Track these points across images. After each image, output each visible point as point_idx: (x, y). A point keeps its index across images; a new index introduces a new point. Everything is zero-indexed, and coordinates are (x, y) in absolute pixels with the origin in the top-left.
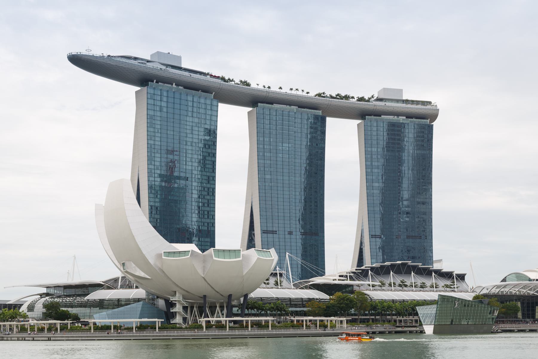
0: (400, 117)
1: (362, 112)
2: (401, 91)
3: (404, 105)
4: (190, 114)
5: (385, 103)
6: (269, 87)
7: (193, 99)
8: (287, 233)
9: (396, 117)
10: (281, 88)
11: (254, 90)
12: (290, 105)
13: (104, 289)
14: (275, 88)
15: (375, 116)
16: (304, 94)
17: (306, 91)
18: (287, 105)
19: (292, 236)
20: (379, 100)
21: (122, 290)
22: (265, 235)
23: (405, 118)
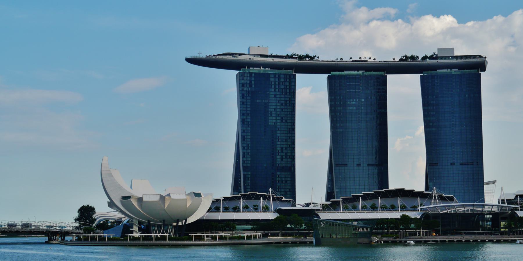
0: (453, 70)
2: (452, 50)
3: (454, 61)
4: (273, 86)
5: (438, 60)
6: (342, 59)
9: (449, 70)
10: (351, 58)
14: (346, 59)
15: (432, 70)
16: (372, 60)
17: (372, 58)
18: (355, 70)
19: (360, 168)
23: (457, 70)
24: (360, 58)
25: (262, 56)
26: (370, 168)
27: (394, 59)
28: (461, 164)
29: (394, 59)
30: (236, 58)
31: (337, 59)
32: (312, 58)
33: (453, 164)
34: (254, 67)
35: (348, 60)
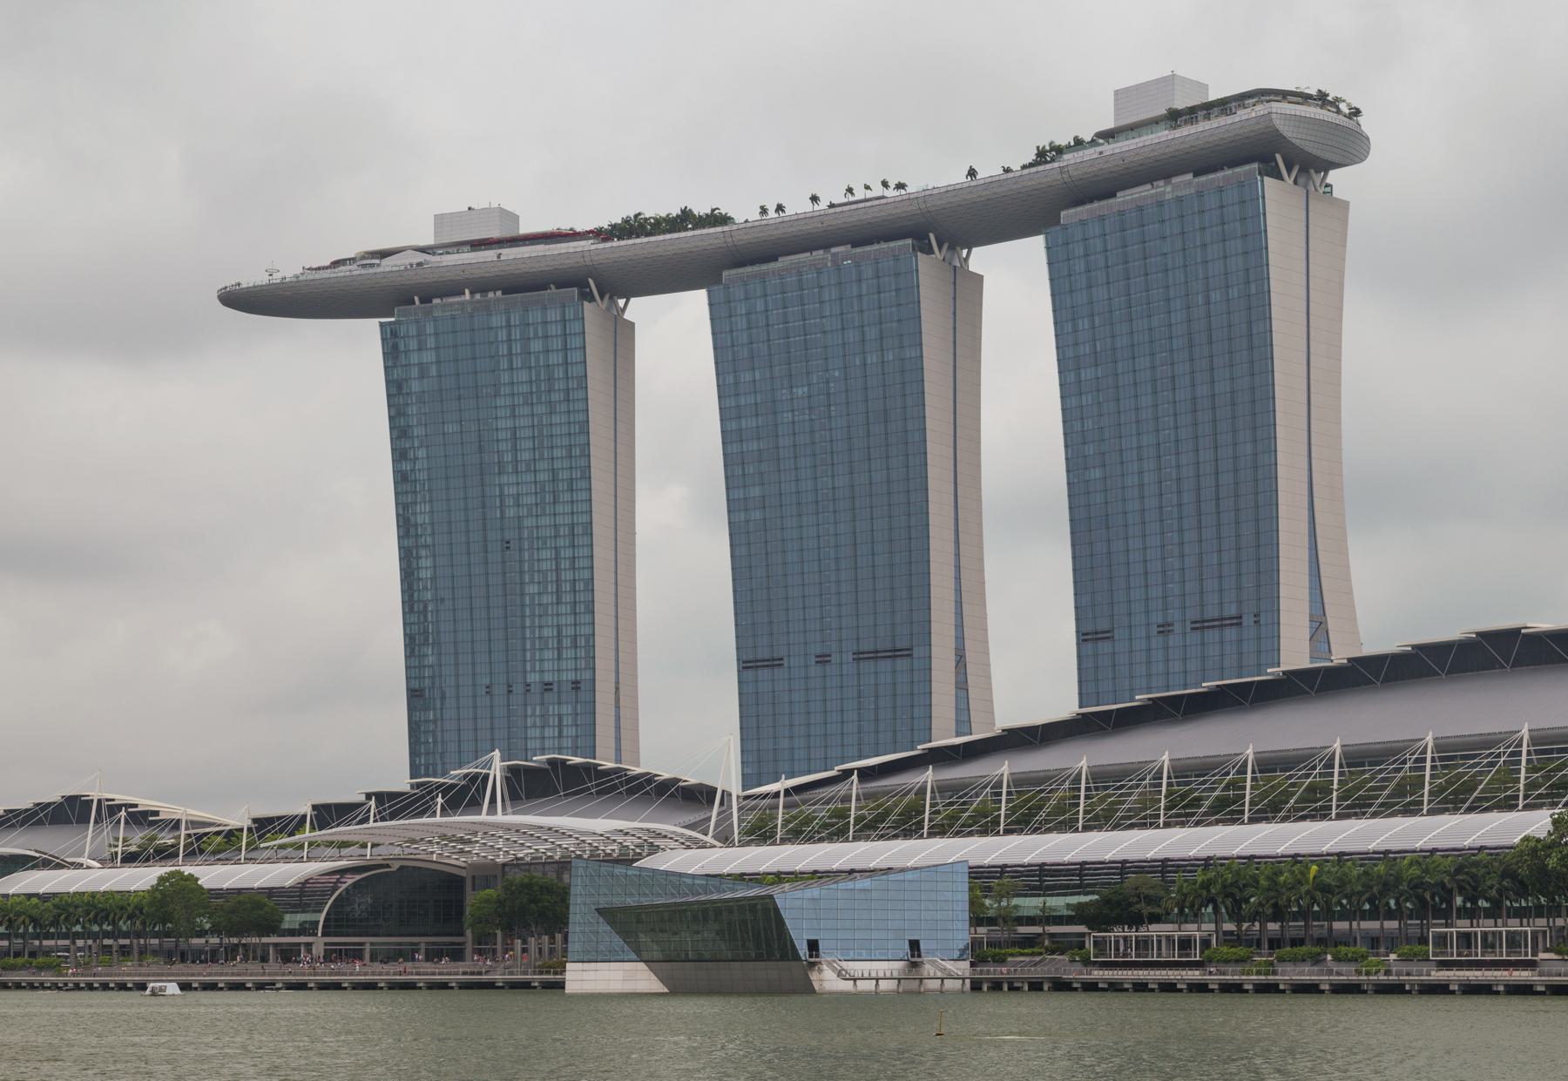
1: (1049, 201)
3: (1163, 135)
7: (508, 320)
8: (813, 660)
10: (814, 199)
11: (748, 226)
12: (826, 246)
13: (33, 868)
14: (798, 206)
16: (891, 193)
17: (892, 185)
18: (810, 249)
19: (828, 666)
20: (1108, 135)
21: (939, 843)
22: (750, 674)
24: (850, 190)
25: (477, 245)
26: (868, 666)
27: (972, 173)
28: (1201, 625)
29: (972, 173)
30: (371, 271)
31: (764, 211)
32: (717, 219)
33: (1165, 629)
34: (441, 296)
35: (754, 215)
